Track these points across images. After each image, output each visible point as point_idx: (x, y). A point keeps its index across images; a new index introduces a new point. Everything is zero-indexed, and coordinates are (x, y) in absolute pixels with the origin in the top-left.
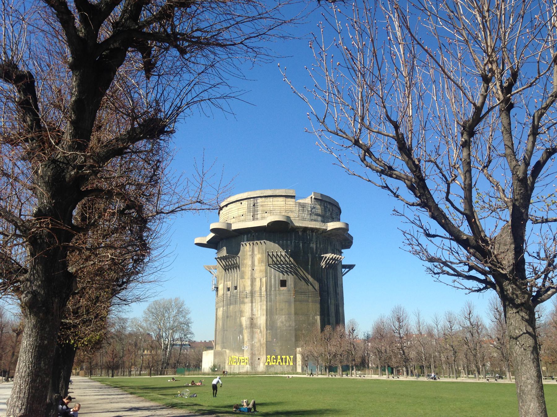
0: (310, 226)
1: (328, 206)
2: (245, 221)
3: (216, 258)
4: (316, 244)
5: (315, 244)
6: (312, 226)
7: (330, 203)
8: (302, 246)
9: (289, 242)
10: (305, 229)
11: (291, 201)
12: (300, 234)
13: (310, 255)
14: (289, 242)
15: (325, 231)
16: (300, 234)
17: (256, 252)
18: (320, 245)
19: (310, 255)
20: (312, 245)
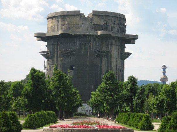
0: (86, 34)
1: (104, 17)
2: (53, 30)
3: (40, 52)
4: (93, 43)
5: (92, 43)
6: (87, 34)
7: (106, 16)
8: (84, 45)
9: (75, 44)
10: (85, 36)
11: (77, 19)
12: (82, 38)
13: (88, 51)
14: (75, 44)
15: (97, 36)
16: (82, 38)
17: (58, 50)
18: (96, 43)
19: (88, 51)
20: (90, 44)
